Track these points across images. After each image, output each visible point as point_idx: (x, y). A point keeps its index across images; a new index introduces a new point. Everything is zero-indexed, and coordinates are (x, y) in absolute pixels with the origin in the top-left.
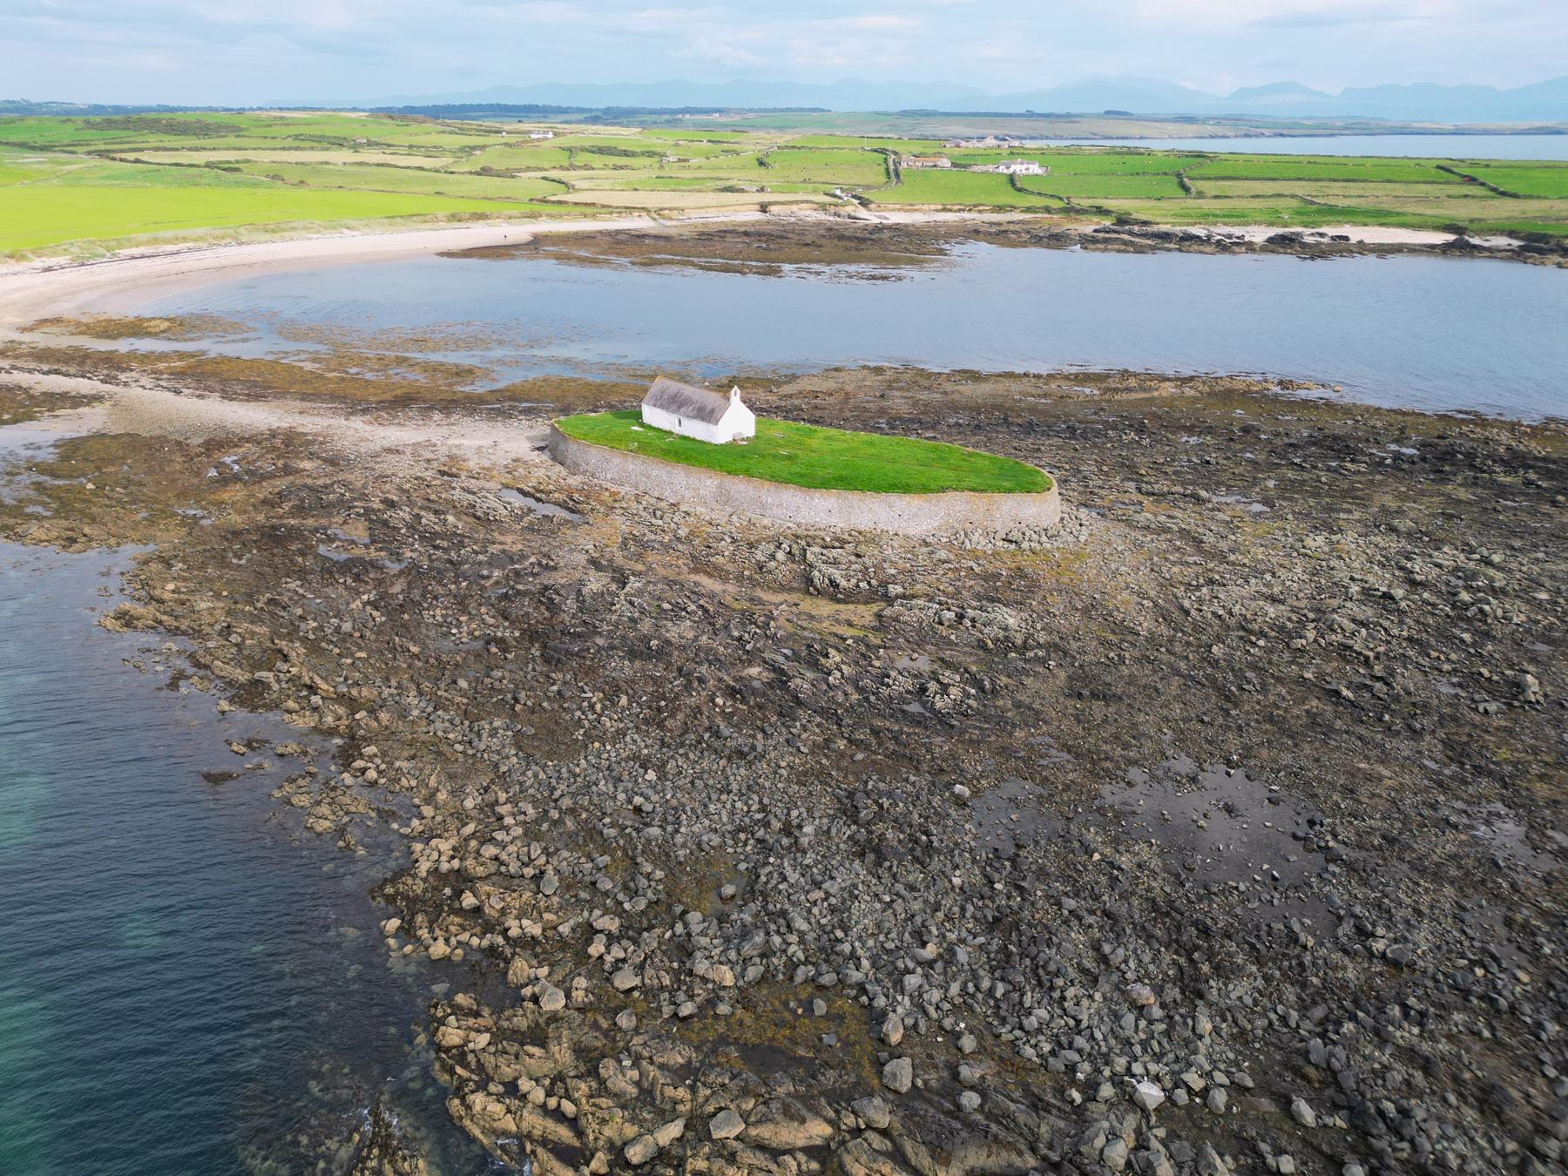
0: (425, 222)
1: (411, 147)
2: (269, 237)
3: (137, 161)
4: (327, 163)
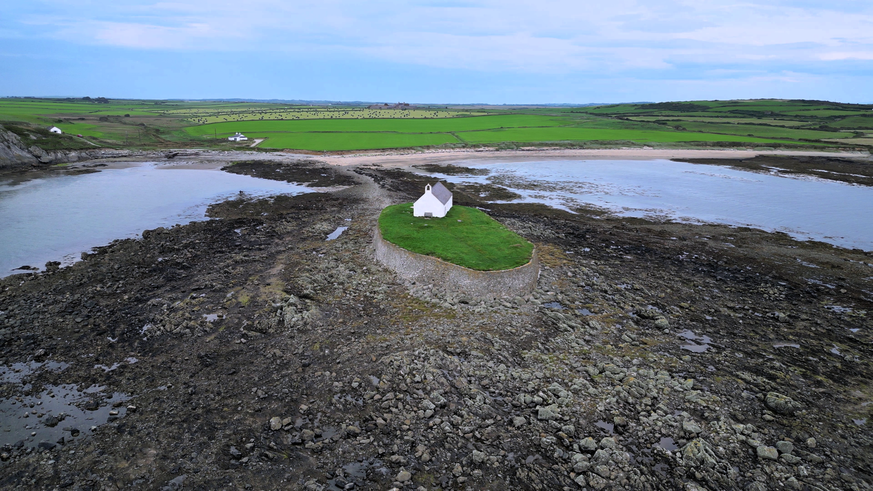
0: (698, 145)
1: (796, 116)
2: (599, 146)
3: (627, 119)
4: (728, 123)
